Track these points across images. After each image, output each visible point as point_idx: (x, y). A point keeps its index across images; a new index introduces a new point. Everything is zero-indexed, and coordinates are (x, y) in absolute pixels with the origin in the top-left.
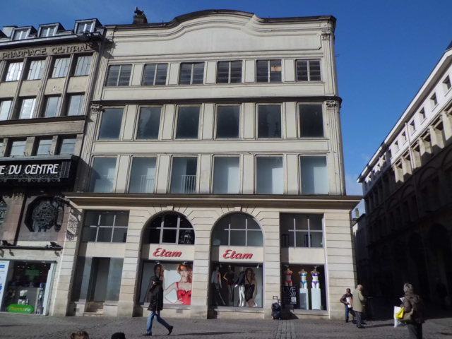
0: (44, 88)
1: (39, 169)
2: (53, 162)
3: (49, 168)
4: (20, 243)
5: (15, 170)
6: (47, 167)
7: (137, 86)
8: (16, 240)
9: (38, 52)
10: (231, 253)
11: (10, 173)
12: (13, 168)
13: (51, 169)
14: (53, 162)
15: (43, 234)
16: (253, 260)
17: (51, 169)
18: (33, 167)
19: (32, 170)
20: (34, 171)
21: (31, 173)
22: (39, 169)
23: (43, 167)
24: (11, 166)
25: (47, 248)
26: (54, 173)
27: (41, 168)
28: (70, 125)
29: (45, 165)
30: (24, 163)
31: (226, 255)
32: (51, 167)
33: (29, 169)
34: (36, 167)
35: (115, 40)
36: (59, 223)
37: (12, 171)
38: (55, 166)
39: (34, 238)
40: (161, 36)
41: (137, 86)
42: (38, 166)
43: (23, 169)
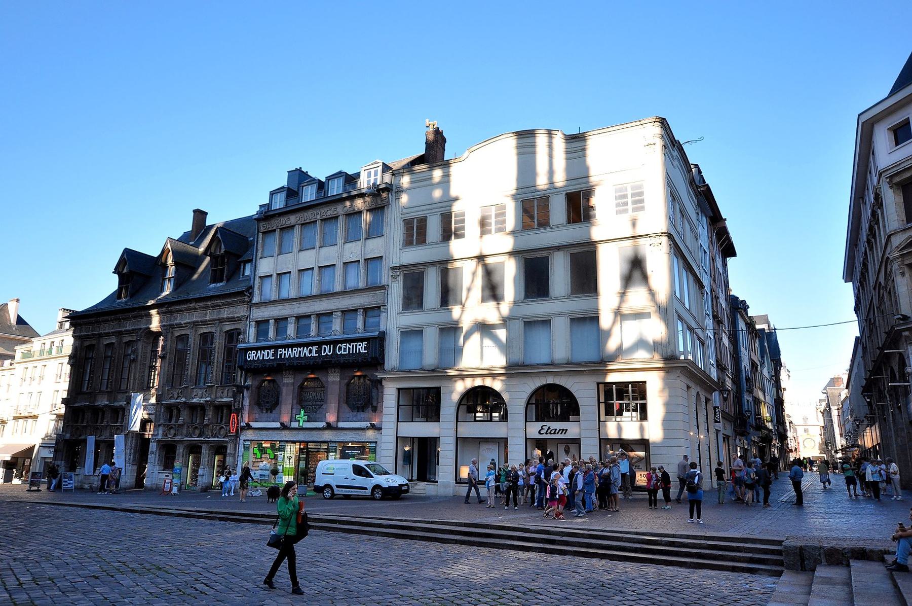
0: (341, 255)
1: (349, 348)
2: (361, 340)
3: (358, 347)
5: (327, 351)
6: (356, 345)
7: (436, 243)
8: (338, 421)
9: (329, 213)
10: (546, 428)
11: (323, 354)
12: (325, 348)
13: (360, 347)
14: (361, 340)
15: (362, 415)
16: (569, 435)
17: (360, 347)
18: (343, 346)
19: (344, 349)
20: (345, 349)
22: (349, 348)
23: (353, 346)
24: (323, 346)
27: (351, 347)
28: (373, 296)
29: (354, 344)
30: (335, 343)
31: (540, 430)
32: (360, 345)
33: (340, 348)
34: (346, 346)
36: (375, 404)
38: (364, 344)
39: (354, 419)
41: (436, 243)
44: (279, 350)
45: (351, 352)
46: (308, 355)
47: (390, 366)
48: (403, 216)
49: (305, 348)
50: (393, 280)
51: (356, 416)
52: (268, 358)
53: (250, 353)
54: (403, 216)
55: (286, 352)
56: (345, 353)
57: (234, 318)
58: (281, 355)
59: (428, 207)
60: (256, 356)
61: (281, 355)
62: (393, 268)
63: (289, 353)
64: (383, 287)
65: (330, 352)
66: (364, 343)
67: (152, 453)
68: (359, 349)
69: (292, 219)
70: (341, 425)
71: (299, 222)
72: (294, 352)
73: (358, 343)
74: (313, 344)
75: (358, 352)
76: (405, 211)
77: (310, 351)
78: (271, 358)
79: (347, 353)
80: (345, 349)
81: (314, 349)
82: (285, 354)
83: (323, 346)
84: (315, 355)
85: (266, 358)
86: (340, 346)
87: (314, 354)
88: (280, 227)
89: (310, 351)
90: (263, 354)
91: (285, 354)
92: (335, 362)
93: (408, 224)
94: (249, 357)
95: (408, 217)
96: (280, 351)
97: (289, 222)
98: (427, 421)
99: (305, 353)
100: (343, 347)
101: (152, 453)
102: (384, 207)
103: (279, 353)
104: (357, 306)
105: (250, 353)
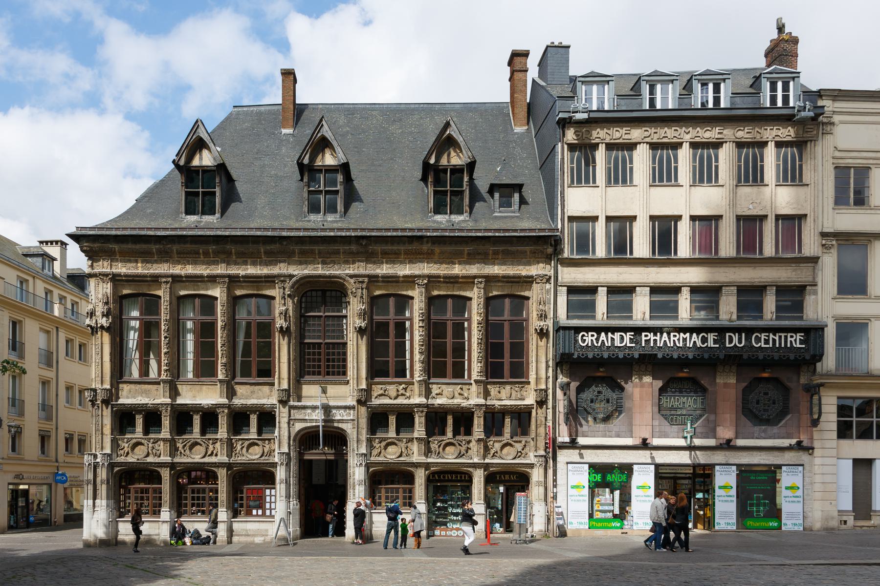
1: (774, 340)
3: (789, 339)
6: (786, 337)
11: (727, 345)
12: (730, 336)
13: (793, 339)
17: (793, 339)
18: (763, 336)
20: (767, 342)
21: (763, 346)
22: (774, 340)
23: (780, 337)
24: (727, 335)
25: (790, 448)
26: (798, 346)
27: (777, 338)
28: (794, 270)
29: (783, 335)
32: (792, 337)
34: (768, 336)
35: (836, 118)
37: (731, 341)
38: (799, 336)
39: (763, 435)
42: (771, 336)
43: (748, 339)
44: (643, 334)
45: (777, 345)
48: (836, 161)
50: (825, 251)
51: (764, 431)
53: (583, 336)
54: (836, 161)
55: (658, 338)
56: (768, 346)
58: (648, 341)
60: (597, 340)
61: (648, 341)
62: (824, 235)
64: (814, 260)
65: (740, 342)
66: (798, 334)
68: (791, 341)
69: (636, 134)
70: (741, 442)
72: (672, 338)
73: (789, 335)
75: (789, 346)
76: (837, 154)
77: (704, 340)
78: (628, 345)
79: (771, 346)
80: (767, 342)
81: (711, 337)
82: (655, 341)
83: (727, 335)
84: (713, 346)
85: (617, 343)
86: (757, 336)
87: (711, 344)
88: (607, 141)
90: (613, 339)
91: (655, 341)
92: (749, 358)
93: (841, 171)
94: (584, 341)
95: (842, 163)
96: (646, 336)
97: (626, 137)
99: (695, 342)
100: (763, 337)
102: (806, 142)
103: (644, 338)
104: (767, 282)
105: (583, 336)
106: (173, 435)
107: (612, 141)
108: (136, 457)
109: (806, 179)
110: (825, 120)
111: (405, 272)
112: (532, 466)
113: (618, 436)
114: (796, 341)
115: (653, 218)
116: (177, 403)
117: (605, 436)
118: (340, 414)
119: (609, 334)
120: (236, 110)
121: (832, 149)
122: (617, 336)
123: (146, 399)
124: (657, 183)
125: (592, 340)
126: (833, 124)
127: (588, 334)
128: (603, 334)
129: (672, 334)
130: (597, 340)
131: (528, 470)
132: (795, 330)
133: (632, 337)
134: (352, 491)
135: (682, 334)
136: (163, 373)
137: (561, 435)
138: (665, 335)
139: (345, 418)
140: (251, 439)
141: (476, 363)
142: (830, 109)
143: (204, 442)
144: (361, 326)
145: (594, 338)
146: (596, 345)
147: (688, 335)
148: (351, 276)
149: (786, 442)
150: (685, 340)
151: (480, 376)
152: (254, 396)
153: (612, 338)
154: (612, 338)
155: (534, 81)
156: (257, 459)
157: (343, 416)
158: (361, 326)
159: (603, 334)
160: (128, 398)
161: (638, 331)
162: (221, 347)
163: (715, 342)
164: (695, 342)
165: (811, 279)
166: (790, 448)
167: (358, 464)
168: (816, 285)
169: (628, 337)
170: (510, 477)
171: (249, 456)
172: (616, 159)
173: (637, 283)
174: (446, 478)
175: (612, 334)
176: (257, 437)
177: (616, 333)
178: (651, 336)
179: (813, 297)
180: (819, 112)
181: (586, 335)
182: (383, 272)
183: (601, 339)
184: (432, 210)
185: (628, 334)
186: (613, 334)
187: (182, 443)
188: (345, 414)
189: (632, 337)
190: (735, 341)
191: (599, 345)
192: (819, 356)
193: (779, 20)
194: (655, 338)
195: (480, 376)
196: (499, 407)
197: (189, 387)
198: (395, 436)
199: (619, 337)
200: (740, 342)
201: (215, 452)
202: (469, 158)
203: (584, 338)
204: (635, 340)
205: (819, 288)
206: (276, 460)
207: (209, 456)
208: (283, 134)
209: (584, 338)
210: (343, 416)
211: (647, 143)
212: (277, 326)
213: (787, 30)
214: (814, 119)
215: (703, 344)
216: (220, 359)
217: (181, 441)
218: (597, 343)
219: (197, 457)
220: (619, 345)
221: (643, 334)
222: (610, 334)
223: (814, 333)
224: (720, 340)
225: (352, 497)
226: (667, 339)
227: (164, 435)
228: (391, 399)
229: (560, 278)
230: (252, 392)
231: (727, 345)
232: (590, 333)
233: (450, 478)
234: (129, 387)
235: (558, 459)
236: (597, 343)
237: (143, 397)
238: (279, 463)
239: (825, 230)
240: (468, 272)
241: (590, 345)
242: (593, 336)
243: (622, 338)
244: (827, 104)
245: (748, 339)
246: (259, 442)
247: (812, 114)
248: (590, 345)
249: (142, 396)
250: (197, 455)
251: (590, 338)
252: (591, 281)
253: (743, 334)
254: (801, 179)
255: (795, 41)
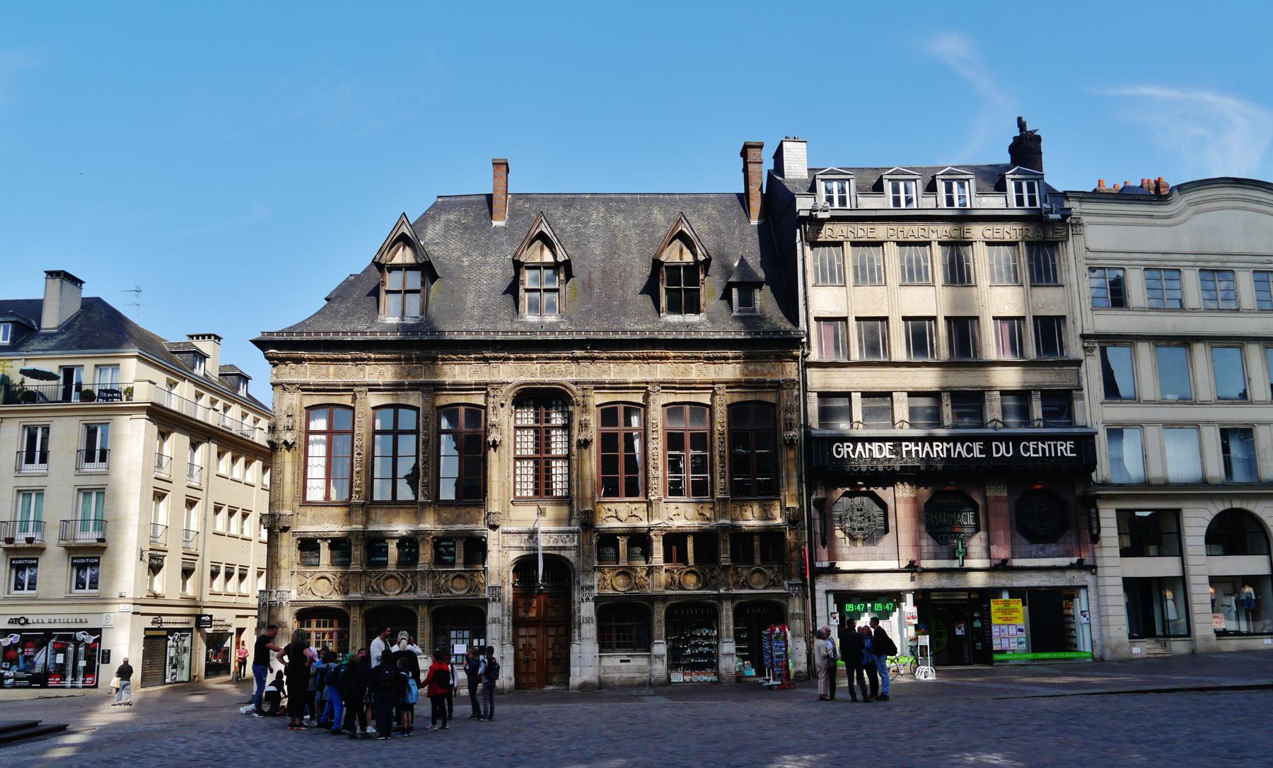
1: (1043, 449)
3: (1059, 448)
4: (1017, 562)
6: (1056, 446)
11: (995, 455)
12: (997, 446)
13: (1063, 448)
17: (1063, 448)
18: (1032, 444)
20: (1036, 451)
21: (1032, 455)
22: (1043, 449)
23: (1049, 446)
26: (1069, 455)
27: (1046, 447)
28: (1058, 374)
29: (1052, 443)
34: (1037, 445)
35: (1085, 219)
37: (998, 451)
38: (1069, 444)
40: (1158, 217)
42: (1040, 444)
44: (904, 444)
46: (964, 454)
47: (1100, 478)
48: (1089, 262)
49: (959, 445)
50: (1088, 353)
52: (883, 456)
53: (838, 447)
54: (1089, 262)
56: (1037, 455)
57: (764, 382)
58: (909, 453)
59: (1126, 256)
61: (909, 453)
62: (1084, 337)
63: (957, 450)
64: (1078, 363)
65: (1008, 452)
66: (1068, 443)
67: (588, 621)
68: (1061, 450)
71: (894, 238)
72: (935, 449)
73: (1059, 443)
74: (973, 438)
75: (1059, 455)
76: (1090, 255)
77: (970, 450)
78: (888, 456)
79: (1041, 455)
80: (1036, 451)
81: (977, 446)
82: (917, 451)
83: (994, 444)
84: (979, 456)
85: (876, 455)
86: (1025, 445)
87: (977, 454)
88: (852, 240)
89: (970, 450)
91: (917, 451)
94: (839, 453)
96: (907, 446)
98: (1160, 555)
99: (959, 452)
100: (1031, 446)
101: (588, 621)
103: (904, 449)
104: (1031, 386)
105: (838, 447)
106: (364, 568)
107: (857, 240)
108: (320, 595)
109: (1063, 277)
110: (1074, 222)
111: (635, 378)
112: (787, 596)
113: (883, 559)
114: (1066, 449)
115: (905, 319)
116: (369, 529)
117: (868, 559)
118: (562, 541)
119: (867, 444)
120: (440, 200)
121: (1084, 250)
122: (875, 446)
123: (333, 526)
124: (907, 283)
125: (848, 452)
126: (1081, 225)
127: (843, 445)
128: (859, 445)
129: (935, 444)
130: (854, 451)
131: (783, 601)
132: (1065, 438)
133: (892, 448)
134: (577, 631)
135: (945, 444)
136: (354, 495)
137: (818, 559)
138: (927, 444)
139: (568, 544)
140: (456, 571)
141: (718, 478)
142: (1078, 210)
143: (401, 576)
144: (585, 439)
145: (850, 450)
146: (852, 456)
147: (951, 444)
148: (576, 383)
149: (1065, 561)
150: (948, 450)
151: (724, 493)
152: (460, 520)
153: (870, 449)
154: (870, 449)
155: (769, 172)
156: (464, 595)
157: (566, 542)
158: (585, 439)
159: (859, 445)
160: (311, 524)
161: (898, 440)
162: (423, 464)
163: (981, 452)
164: (959, 452)
165: (1076, 384)
166: (1071, 567)
167: (584, 598)
168: (1082, 389)
169: (887, 447)
170: (761, 609)
171: (454, 591)
172: (862, 258)
173: (895, 388)
174: (688, 613)
175: (869, 444)
176: (463, 569)
177: (873, 443)
178: (912, 446)
179: (1081, 402)
180: (1066, 213)
181: (841, 446)
182: (609, 378)
183: (858, 450)
184: (664, 310)
185: (887, 444)
186: (870, 444)
187: (375, 577)
188: (567, 540)
189: (892, 448)
190: (1002, 451)
191: (856, 456)
192: (1092, 465)
193: (1019, 119)
194: (917, 448)
195: (724, 493)
196: (746, 528)
197: (383, 511)
198: (626, 564)
199: (877, 447)
200: (1008, 452)
201: (413, 588)
202: (704, 255)
203: (839, 449)
204: (896, 451)
205: (1085, 392)
206: (487, 596)
207: (406, 592)
208: (493, 226)
209: (839, 449)
210: (566, 542)
211: (894, 242)
212: (489, 439)
213: (1029, 128)
214: (1063, 221)
215: (969, 454)
216: (421, 478)
217: (373, 575)
218: (854, 455)
219: (391, 593)
220: (878, 456)
221: (904, 444)
222: (867, 444)
223: (1085, 442)
224: (986, 450)
225: (577, 638)
226: (929, 450)
227: (353, 568)
228: (622, 521)
229: (809, 383)
230: (457, 516)
231: (995, 455)
232: (845, 444)
233: (692, 612)
234: (313, 513)
235: (817, 587)
236: (854, 455)
237: (330, 524)
238: (491, 599)
239: (1085, 332)
240: (706, 378)
241: (846, 457)
242: (848, 447)
243: (880, 449)
244: (1074, 206)
245: (1016, 448)
246: (467, 575)
247: (1058, 216)
248: (846, 457)
249: (328, 522)
250: (392, 591)
251: (846, 449)
252: (843, 386)
253: (1011, 443)
254: (1055, 280)
255: (1038, 139)
